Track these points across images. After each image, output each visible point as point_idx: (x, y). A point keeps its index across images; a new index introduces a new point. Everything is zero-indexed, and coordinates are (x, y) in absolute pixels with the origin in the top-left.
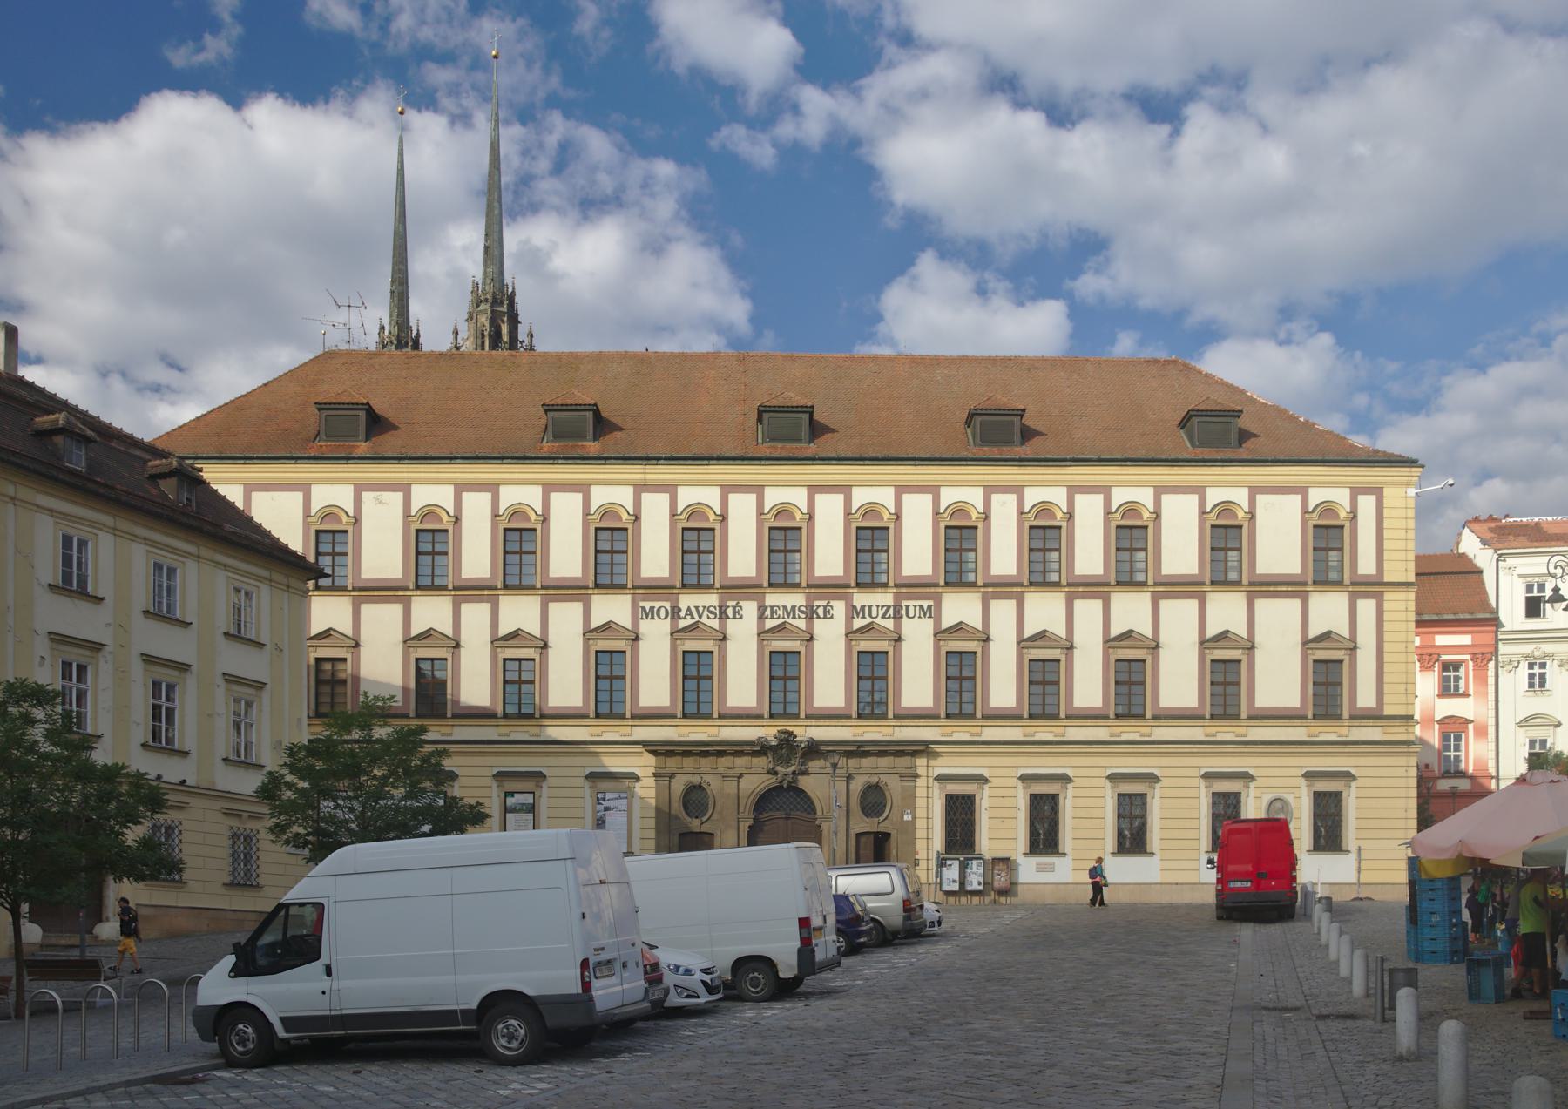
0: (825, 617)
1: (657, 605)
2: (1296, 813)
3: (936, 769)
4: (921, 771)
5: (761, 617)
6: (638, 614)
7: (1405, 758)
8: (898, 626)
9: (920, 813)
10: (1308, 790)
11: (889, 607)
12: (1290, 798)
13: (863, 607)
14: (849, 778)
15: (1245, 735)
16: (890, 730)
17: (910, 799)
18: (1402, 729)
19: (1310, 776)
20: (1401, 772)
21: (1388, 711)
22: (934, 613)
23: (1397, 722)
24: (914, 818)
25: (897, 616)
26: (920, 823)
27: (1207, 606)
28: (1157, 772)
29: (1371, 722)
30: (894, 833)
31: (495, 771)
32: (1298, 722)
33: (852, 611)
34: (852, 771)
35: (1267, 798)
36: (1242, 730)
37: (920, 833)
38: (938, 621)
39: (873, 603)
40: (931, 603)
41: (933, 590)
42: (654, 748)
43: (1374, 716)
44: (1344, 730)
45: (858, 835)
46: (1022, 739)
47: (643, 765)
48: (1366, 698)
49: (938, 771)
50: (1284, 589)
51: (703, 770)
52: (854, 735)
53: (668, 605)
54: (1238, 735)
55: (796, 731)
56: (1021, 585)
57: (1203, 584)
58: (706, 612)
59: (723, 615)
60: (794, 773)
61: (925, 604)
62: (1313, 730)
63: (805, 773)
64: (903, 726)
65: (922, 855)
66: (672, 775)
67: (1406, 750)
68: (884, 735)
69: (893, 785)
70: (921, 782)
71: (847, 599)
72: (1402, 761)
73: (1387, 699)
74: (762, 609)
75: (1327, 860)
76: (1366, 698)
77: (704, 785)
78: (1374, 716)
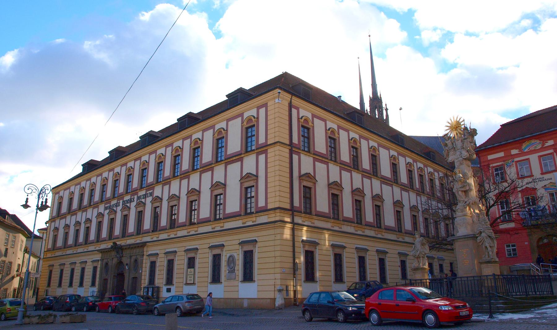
0: (133, 202)
1: (107, 205)
2: (237, 262)
3: (149, 252)
4: (145, 253)
5: (123, 205)
6: (106, 208)
7: (273, 230)
8: (145, 201)
9: (144, 269)
10: (242, 251)
11: (144, 195)
12: (235, 255)
13: (140, 196)
14: (131, 257)
15: (223, 227)
16: (141, 239)
17: (142, 263)
18: (274, 215)
19: (242, 243)
20: (272, 237)
21: (269, 207)
22: (151, 194)
23: (272, 212)
24: (142, 271)
25: (145, 198)
26: (143, 273)
27: (214, 172)
28: (197, 247)
29: (262, 214)
30: (138, 277)
31: (70, 263)
32: (238, 218)
33: (139, 198)
34: (132, 255)
35: (228, 256)
36: (222, 225)
37: (143, 277)
38: (153, 197)
39: (142, 195)
40: (152, 191)
41: (152, 186)
42: (102, 251)
43: (265, 210)
44: (254, 219)
45: (133, 278)
46: (167, 238)
47: (98, 257)
48: (261, 203)
49: (150, 252)
50: (235, 159)
51: (108, 257)
52: (135, 241)
53: (109, 205)
54: (221, 227)
55: (118, 243)
56: (170, 179)
57: (212, 164)
58: (115, 206)
59: (117, 206)
60: (120, 256)
61: (151, 191)
62: (245, 220)
63: (123, 256)
64: (144, 236)
65: (142, 286)
66: (103, 260)
67: (273, 226)
68: (140, 240)
69: (139, 258)
70: (145, 257)
71: (137, 194)
72: (271, 232)
73: (269, 200)
74: (123, 202)
75: (248, 285)
76: (261, 203)
77: (108, 262)
78: (265, 210)
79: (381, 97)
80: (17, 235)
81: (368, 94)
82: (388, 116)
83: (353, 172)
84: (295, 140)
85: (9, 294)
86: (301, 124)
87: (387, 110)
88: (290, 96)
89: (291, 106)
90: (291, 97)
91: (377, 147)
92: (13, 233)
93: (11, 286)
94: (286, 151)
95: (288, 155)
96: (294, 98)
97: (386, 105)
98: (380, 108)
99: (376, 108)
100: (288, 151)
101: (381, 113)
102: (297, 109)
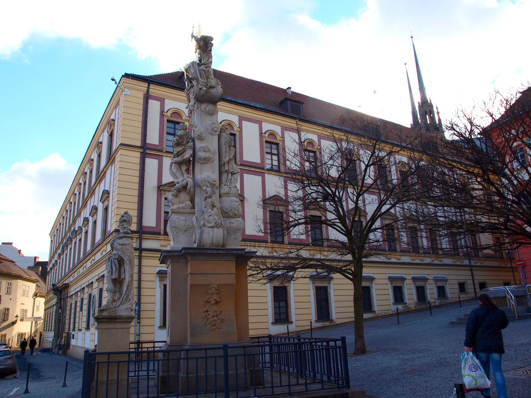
79: (430, 101)
80: (14, 282)
81: (417, 99)
82: (440, 120)
83: (266, 175)
84: (153, 138)
85: (9, 339)
86: (166, 119)
87: (438, 113)
88: (146, 85)
89: (147, 97)
90: (147, 86)
91: (316, 141)
92: (6, 280)
93: (12, 331)
94: (135, 156)
95: (138, 161)
96: (152, 86)
97: (437, 108)
98: (431, 112)
99: (426, 113)
100: (138, 155)
101: (432, 119)
102: (162, 101)
